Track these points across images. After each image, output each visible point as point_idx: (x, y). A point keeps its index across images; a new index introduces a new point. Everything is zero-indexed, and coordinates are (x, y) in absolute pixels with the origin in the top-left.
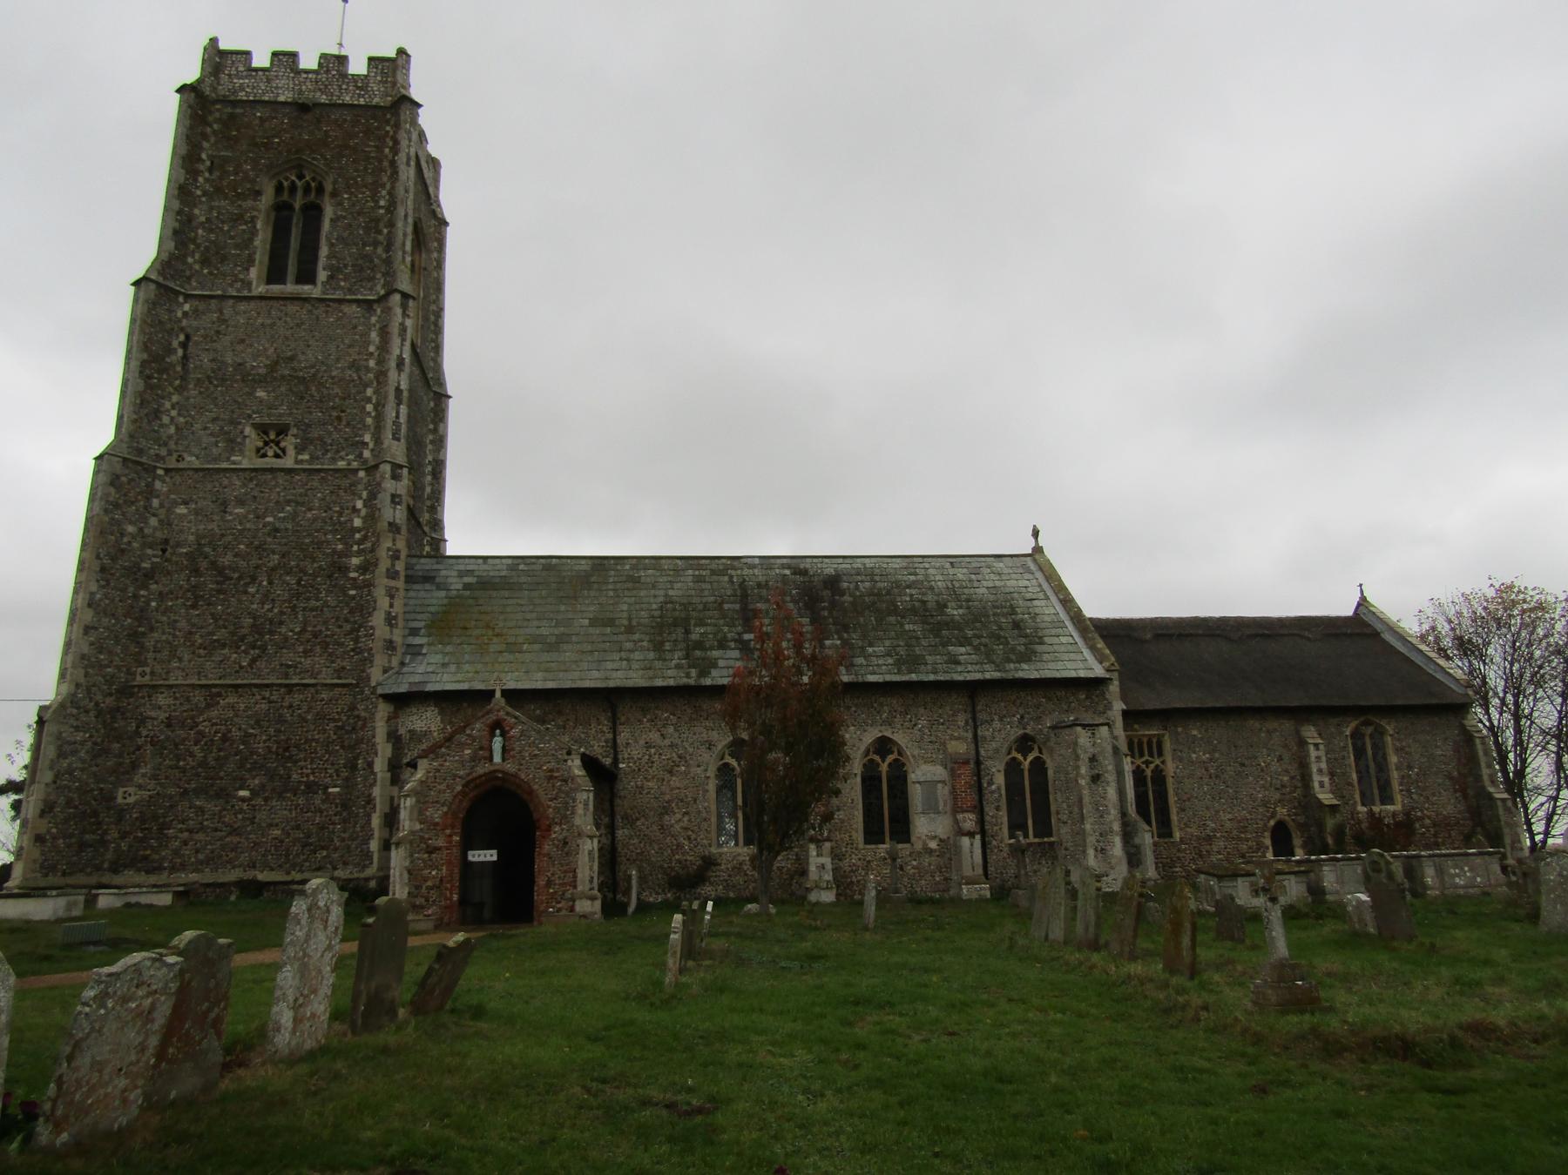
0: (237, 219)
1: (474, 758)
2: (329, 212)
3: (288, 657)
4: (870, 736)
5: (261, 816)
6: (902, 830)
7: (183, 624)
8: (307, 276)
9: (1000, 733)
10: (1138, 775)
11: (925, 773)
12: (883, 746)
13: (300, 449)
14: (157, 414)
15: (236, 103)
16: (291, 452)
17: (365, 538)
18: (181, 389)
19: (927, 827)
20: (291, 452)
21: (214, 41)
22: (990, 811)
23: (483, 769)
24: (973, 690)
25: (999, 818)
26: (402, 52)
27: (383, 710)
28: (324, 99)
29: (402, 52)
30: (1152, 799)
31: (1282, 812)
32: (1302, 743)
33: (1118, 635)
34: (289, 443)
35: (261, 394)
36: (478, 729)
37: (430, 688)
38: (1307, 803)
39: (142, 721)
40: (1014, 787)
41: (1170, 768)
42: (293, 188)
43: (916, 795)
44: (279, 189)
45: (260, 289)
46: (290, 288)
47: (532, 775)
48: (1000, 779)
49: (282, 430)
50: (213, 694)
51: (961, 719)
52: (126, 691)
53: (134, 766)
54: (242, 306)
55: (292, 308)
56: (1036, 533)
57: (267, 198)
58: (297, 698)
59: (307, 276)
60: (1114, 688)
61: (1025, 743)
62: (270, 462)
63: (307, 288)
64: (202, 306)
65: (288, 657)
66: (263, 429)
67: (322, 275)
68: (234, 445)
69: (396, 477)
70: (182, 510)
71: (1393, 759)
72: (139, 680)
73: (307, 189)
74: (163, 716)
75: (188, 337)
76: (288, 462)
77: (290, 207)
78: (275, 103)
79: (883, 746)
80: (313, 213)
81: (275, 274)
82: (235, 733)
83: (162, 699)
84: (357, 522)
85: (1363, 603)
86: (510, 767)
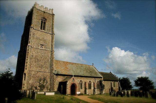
4: (89, 81)
7: (34, 64)
8: (44, 29)
11: (92, 84)
12: (90, 81)
13: (45, 48)
15: (38, 9)
18: (34, 39)
23: (72, 82)
24: (95, 77)
28: (46, 12)
32: (111, 83)
33: (102, 74)
35: (41, 41)
38: (112, 88)
39: (31, 74)
42: (43, 20)
44: (42, 20)
46: (43, 31)
50: (38, 72)
51: (94, 79)
53: (31, 79)
54: (39, 31)
56: (93, 64)
57: (41, 21)
58: (45, 73)
60: (103, 78)
62: (41, 48)
64: (35, 30)
65: (44, 69)
66: (41, 45)
67: (46, 30)
70: (34, 52)
74: (33, 74)
75: (34, 34)
79: (90, 81)
80: (45, 23)
81: (41, 29)
82: (40, 76)
83: (33, 72)
84: (50, 56)
85: (110, 72)
86: (74, 82)
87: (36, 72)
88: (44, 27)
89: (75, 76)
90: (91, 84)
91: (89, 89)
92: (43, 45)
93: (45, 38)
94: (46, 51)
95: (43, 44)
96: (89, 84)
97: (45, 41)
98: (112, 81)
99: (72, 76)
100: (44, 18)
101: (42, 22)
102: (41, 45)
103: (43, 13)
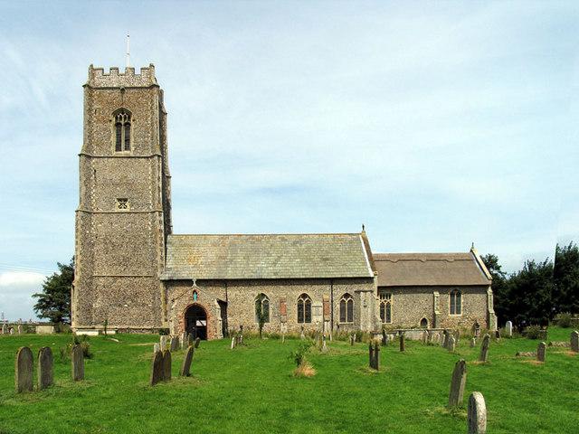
0: (105, 130)
1: (190, 300)
2: (133, 126)
3: (134, 268)
5: (131, 311)
6: (309, 320)
8: (127, 148)
9: (340, 291)
10: (382, 306)
11: (317, 304)
13: (131, 206)
14: (90, 196)
16: (128, 207)
17: (152, 235)
19: (317, 318)
20: (128, 207)
21: (92, 66)
22: (334, 314)
23: (192, 302)
24: (332, 281)
25: (337, 317)
26: (152, 66)
27: (161, 285)
28: (128, 85)
29: (152, 66)
30: (385, 312)
31: (425, 316)
34: (127, 204)
36: (190, 292)
37: (175, 278)
40: (342, 310)
41: (392, 303)
43: (313, 310)
45: (114, 154)
46: (123, 153)
47: (204, 304)
48: (338, 306)
49: (126, 200)
52: (92, 277)
55: (125, 160)
58: (137, 280)
59: (127, 148)
61: (347, 295)
63: (128, 152)
66: (119, 200)
67: (133, 148)
68: (112, 205)
69: (160, 215)
71: (462, 301)
72: (95, 275)
73: (125, 118)
76: (129, 211)
77: (120, 124)
78: (113, 88)
80: (127, 125)
81: (118, 148)
86: (199, 302)
87: (111, 279)
88: (127, 140)
89: (200, 282)
90: (309, 305)
91: (300, 320)
92: (126, 200)
93: (131, 176)
94: (137, 215)
95: (125, 195)
96: (300, 306)
97: (130, 185)
98: (442, 288)
99: (188, 282)
100: (122, 111)
101: (118, 125)
102: (119, 200)
103: (117, 93)
